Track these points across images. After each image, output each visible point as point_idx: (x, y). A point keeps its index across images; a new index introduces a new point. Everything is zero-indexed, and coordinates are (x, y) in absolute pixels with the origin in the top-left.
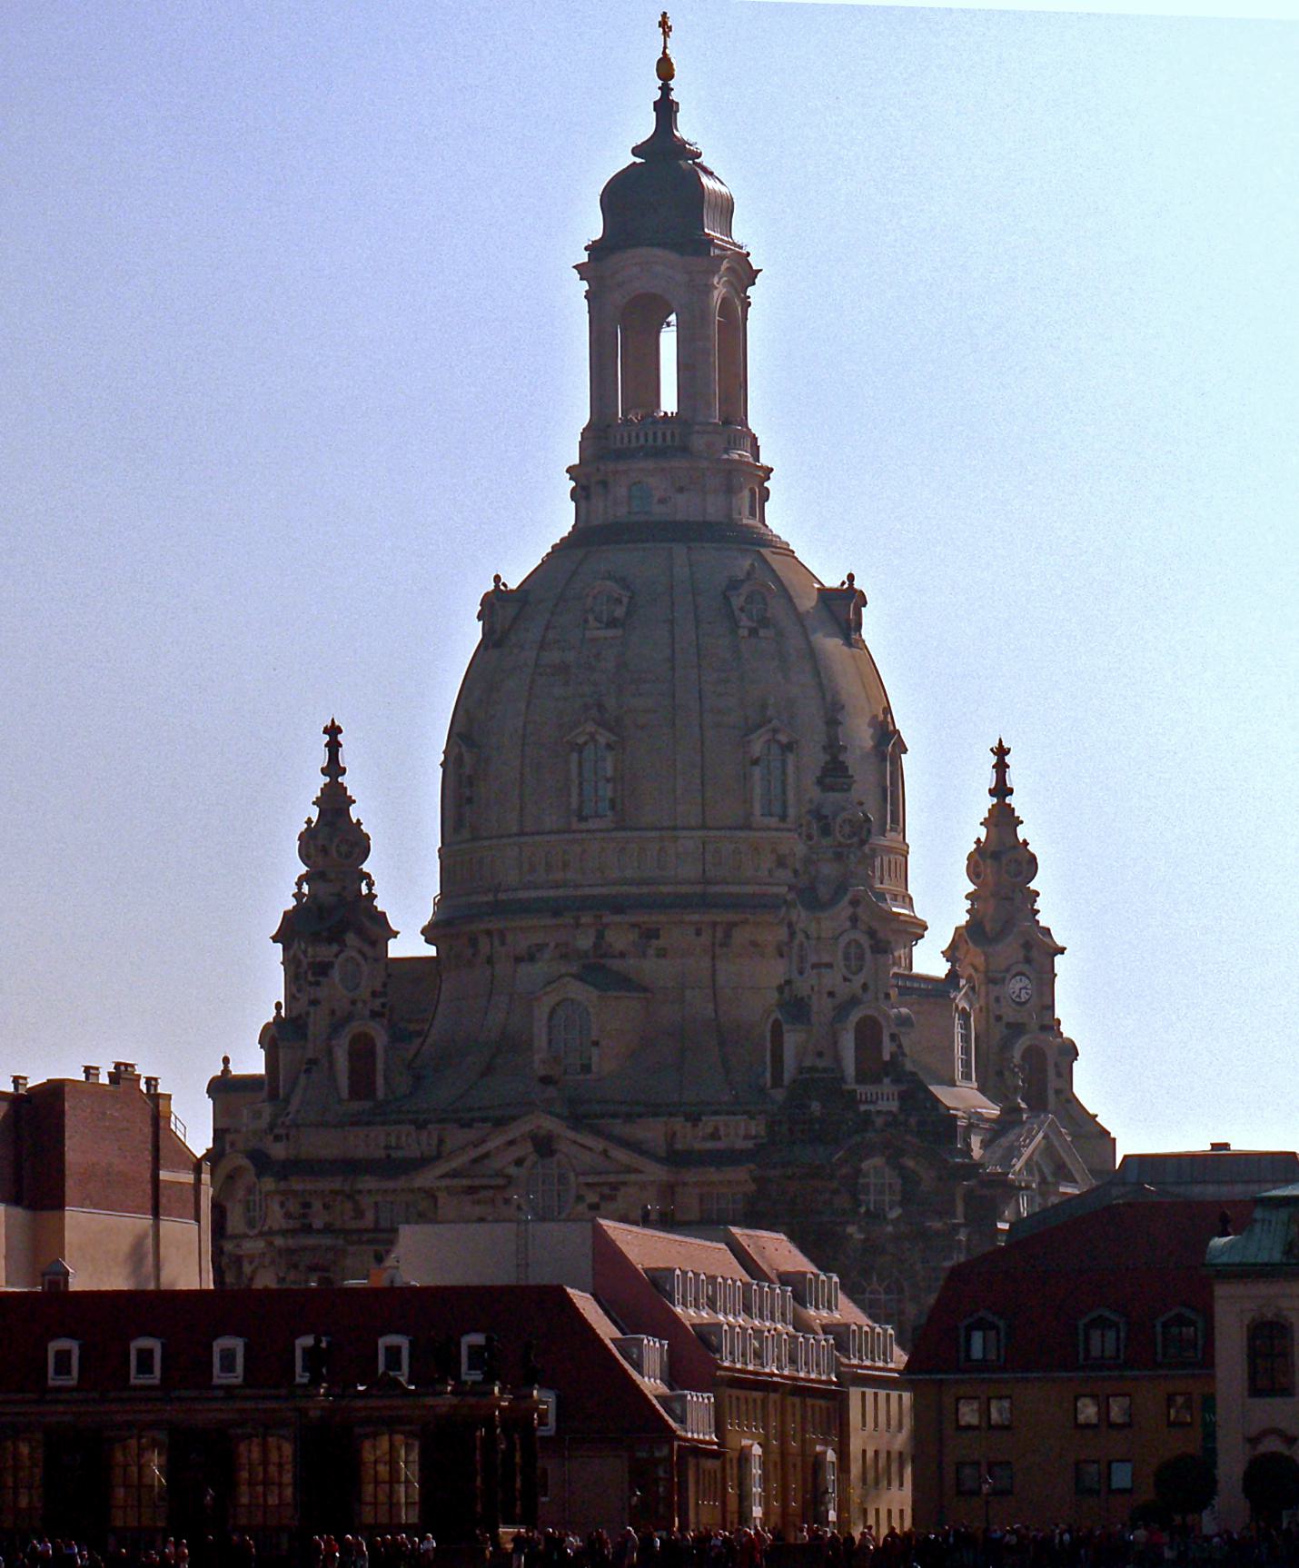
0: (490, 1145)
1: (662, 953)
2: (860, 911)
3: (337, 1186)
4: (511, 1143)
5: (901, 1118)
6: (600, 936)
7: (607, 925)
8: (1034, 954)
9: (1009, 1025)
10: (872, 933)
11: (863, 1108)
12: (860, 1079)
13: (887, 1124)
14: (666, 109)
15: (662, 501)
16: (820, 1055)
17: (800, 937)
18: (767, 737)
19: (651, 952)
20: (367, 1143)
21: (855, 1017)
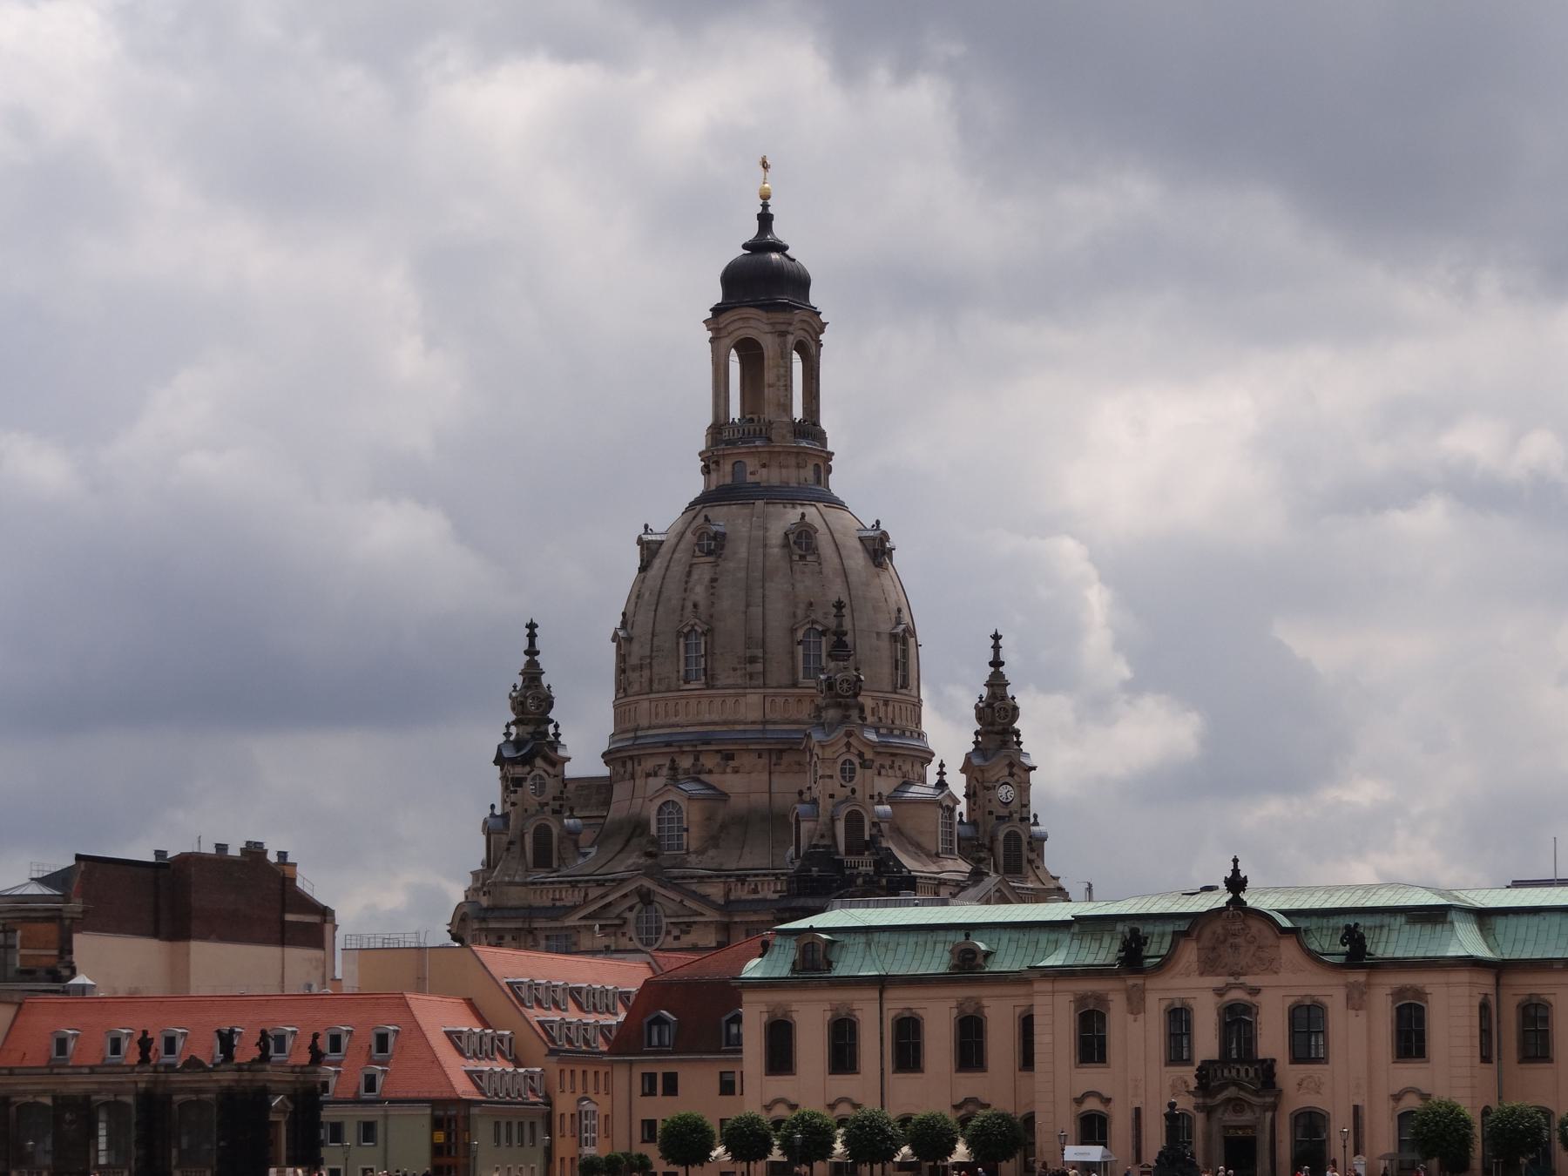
0: (610, 898)
1: (736, 771)
2: (852, 740)
3: (519, 925)
4: (625, 896)
6: (697, 759)
8: (1015, 770)
9: (998, 818)
10: (861, 755)
12: (848, 852)
14: (765, 220)
16: (822, 836)
19: (729, 770)
20: (542, 900)
21: (843, 812)
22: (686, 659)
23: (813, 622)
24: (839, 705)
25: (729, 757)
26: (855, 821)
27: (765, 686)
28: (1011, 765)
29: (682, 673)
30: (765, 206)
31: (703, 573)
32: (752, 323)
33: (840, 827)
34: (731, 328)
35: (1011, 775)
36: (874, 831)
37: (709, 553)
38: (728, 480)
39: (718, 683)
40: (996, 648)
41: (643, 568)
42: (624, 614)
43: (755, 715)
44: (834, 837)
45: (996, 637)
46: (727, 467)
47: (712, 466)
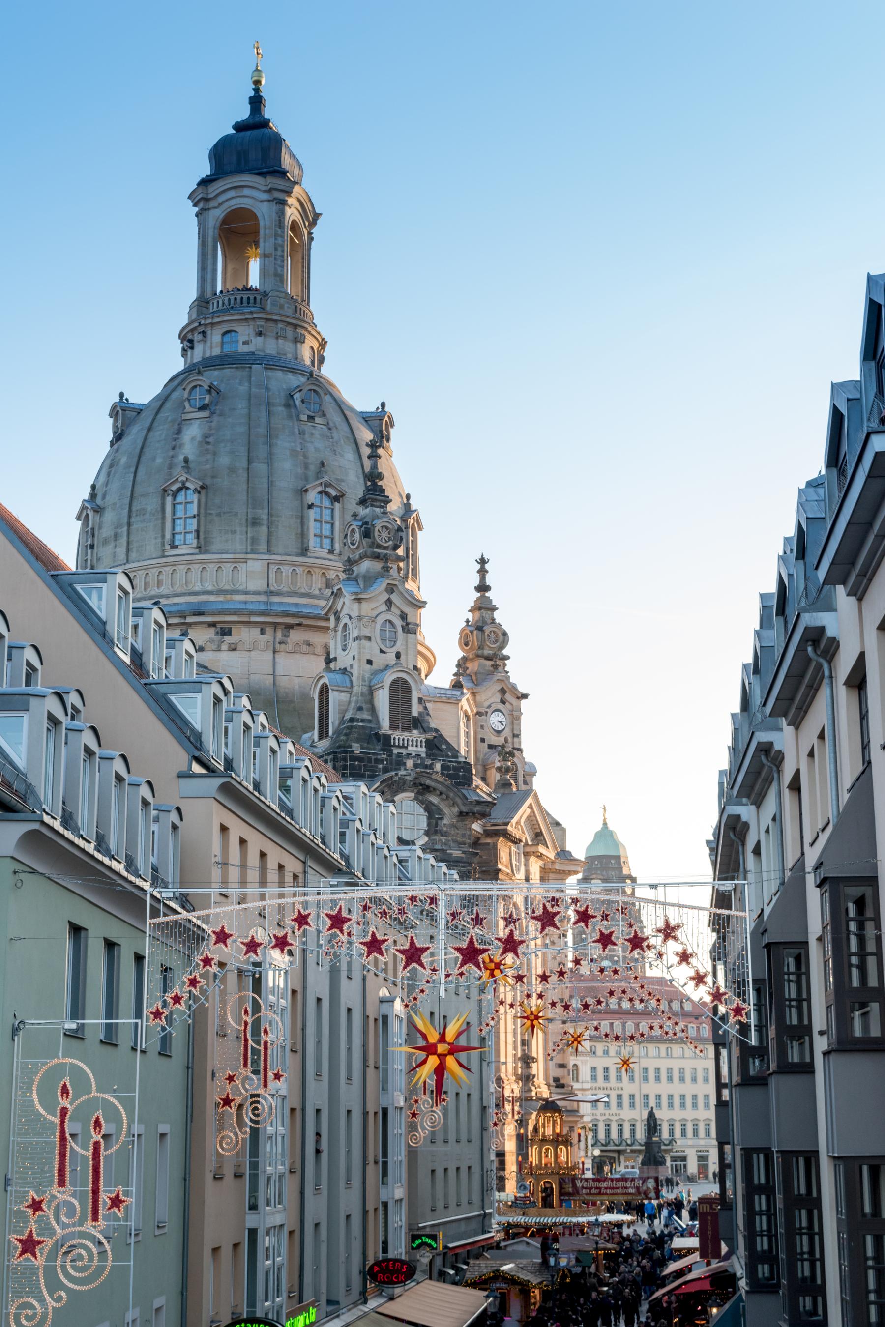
2: (394, 597)
5: (428, 762)
7: (189, 625)
8: (508, 696)
9: (490, 747)
10: (403, 616)
11: (396, 751)
12: (393, 727)
13: (416, 766)
14: (256, 102)
15: (245, 343)
16: (360, 709)
17: (345, 620)
18: (320, 489)
19: (224, 647)
21: (389, 678)
22: (174, 520)
23: (327, 485)
24: (377, 557)
25: (226, 632)
26: (401, 691)
27: (269, 552)
28: (503, 691)
29: (168, 536)
30: (257, 90)
31: (193, 432)
32: (246, 191)
33: (382, 699)
34: (221, 199)
35: (503, 702)
36: (421, 709)
37: (203, 408)
38: (217, 351)
39: (214, 548)
40: (483, 572)
41: (118, 437)
42: (93, 487)
43: (257, 584)
44: (373, 710)
45: (483, 561)
46: (215, 336)
47: (197, 337)
